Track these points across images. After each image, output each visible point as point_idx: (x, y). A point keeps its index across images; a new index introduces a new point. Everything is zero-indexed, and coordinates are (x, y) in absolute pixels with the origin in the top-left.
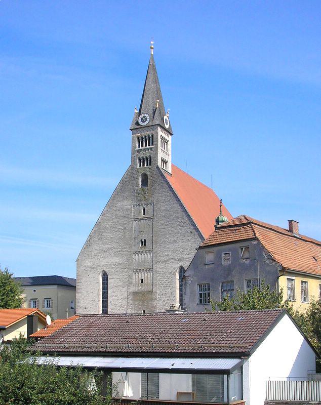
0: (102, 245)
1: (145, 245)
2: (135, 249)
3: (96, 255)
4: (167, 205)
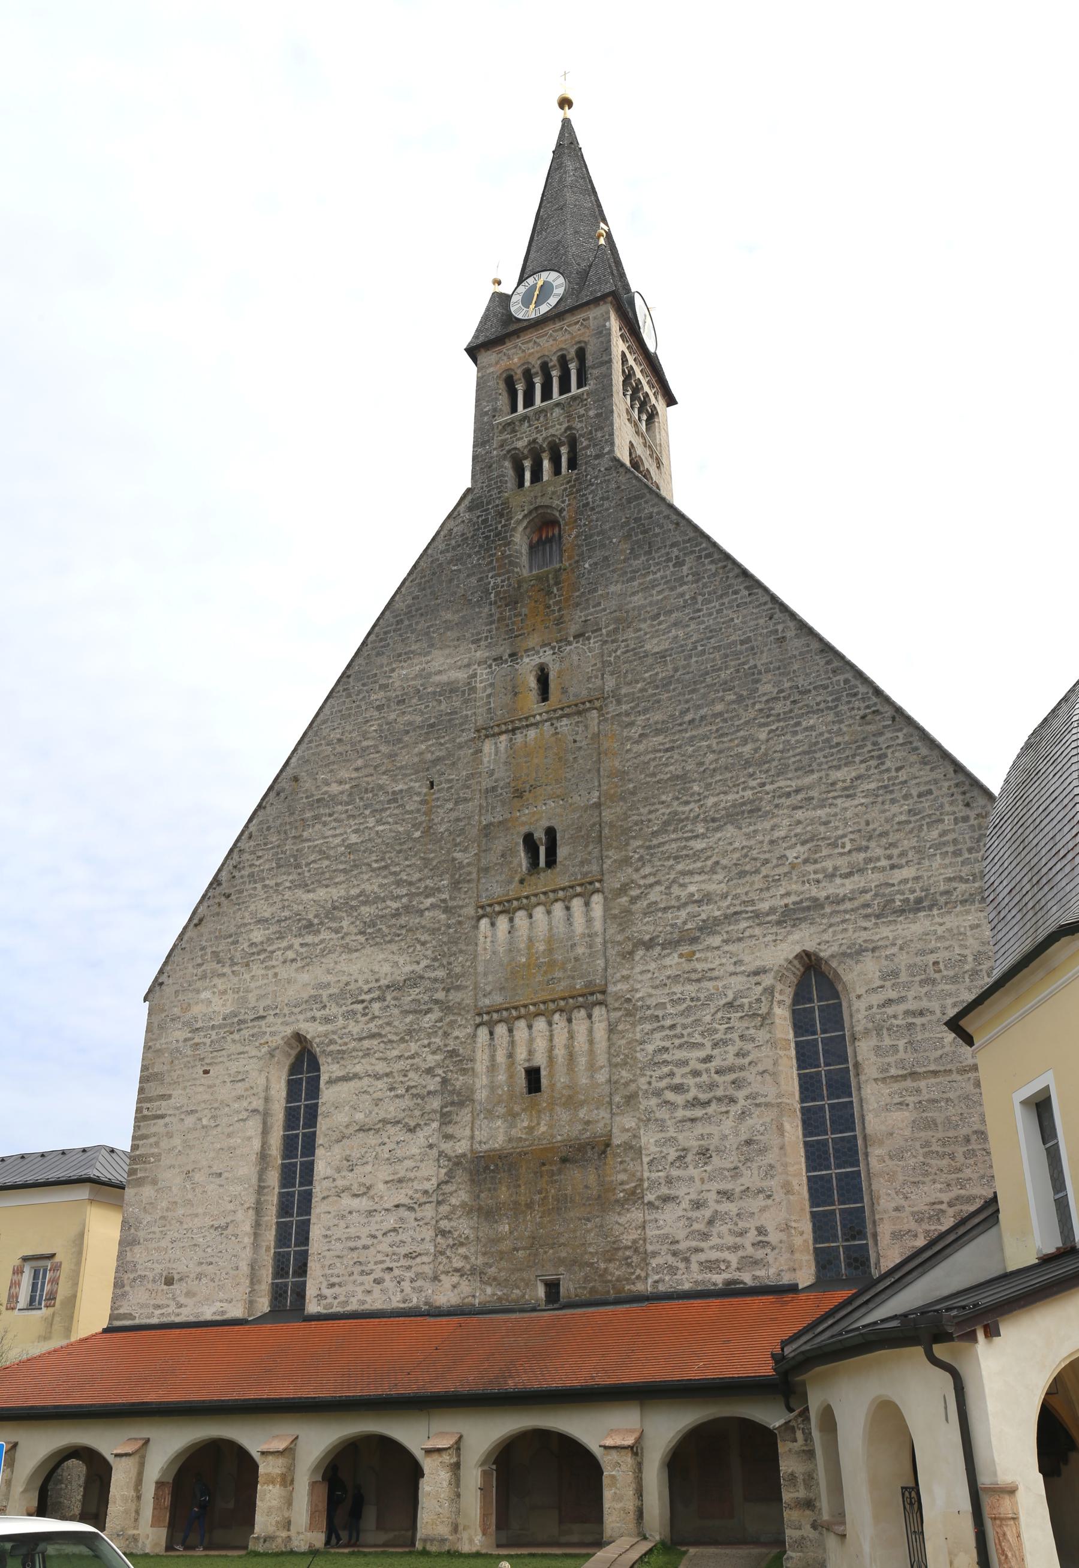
0: (299, 893)
1: (551, 862)
2: (495, 888)
3: (259, 950)
4: (675, 624)
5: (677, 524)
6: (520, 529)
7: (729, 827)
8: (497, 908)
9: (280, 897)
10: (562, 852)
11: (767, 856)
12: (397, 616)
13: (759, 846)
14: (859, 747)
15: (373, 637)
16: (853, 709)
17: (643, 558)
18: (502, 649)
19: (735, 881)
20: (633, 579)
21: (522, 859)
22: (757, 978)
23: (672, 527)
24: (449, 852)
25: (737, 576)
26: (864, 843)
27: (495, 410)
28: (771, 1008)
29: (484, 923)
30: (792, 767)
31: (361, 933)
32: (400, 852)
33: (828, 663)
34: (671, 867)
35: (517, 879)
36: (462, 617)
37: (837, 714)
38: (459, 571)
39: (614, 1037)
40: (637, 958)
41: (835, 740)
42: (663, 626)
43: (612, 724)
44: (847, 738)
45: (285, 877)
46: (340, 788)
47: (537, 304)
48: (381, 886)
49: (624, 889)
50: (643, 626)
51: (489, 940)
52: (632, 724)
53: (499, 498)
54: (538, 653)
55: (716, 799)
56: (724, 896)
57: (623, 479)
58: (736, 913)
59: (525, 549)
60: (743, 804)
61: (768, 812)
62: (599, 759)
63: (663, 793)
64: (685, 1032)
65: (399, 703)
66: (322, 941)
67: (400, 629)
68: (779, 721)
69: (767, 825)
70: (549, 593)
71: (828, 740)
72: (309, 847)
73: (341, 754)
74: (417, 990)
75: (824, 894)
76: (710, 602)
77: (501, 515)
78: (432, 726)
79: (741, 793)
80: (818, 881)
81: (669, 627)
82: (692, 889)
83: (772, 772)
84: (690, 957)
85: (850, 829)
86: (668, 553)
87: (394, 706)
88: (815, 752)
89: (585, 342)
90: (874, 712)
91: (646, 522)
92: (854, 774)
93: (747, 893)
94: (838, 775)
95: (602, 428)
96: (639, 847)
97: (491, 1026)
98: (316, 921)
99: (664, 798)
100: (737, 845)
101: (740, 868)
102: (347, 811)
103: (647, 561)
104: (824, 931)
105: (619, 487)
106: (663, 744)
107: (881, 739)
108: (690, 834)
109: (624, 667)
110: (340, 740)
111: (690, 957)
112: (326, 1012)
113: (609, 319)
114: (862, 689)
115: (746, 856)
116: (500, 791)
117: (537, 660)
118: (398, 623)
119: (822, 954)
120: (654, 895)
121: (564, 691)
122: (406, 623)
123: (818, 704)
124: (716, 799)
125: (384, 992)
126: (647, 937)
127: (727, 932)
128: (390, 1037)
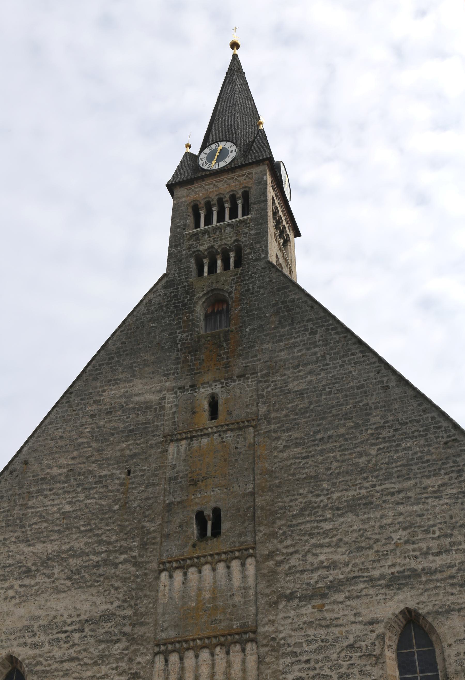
0: (22, 546)
1: (216, 532)
2: (173, 549)
4: (310, 373)
5: (312, 307)
6: (200, 303)
7: (350, 515)
8: (175, 565)
9: (6, 548)
10: (225, 526)
11: (378, 537)
12: (109, 354)
13: (372, 529)
14: (443, 464)
15: (90, 367)
16: (438, 437)
17: (288, 327)
18: (185, 381)
19: (354, 554)
20: (280, 341)
21: (194, 529)
22: (372, 627)
23: (308, 308)
24: (139, 521)
25: (354, 344)
26: (449, 531)
27: (185, 225)
28: (383, 650)
29: (164, 575)
30: (395, 475)
31: (69, 578)
32: (102, 520)
33: (420, 405)
34: (307, 541)
35: (191, 543)
36: (157, 358)
37: (427, 440)
38: (156, 327)
39: (263, 667)
40: (281, 607)
41: (426, 458)
42: (301, 374)
43: (264, 437)
44: (434, 457)
45: (12, 534)
46: (60, 471)
47: (218, 161)
48: (86, 544)
49: (271, 555)
50: (287, 372)
51: (167, 588)
52: (278, 438)
53: (186, 282)
54: (211, 386)
55: (339, 494)
56: (346, 564)
57: (274, 275)
58: (355, 577)
59: (202, 317)
60: (360, 498)
61: (378, 505)
62: (254, 461)
63: (301, 488)
64: (317, 666)
65: (107, 414)
66: (37, 584)
67: (111, 363)
68: (385, 442)
69: (378, 514)
70: (220, 346)
71: (421, 458)
72: (32, 513)
73: (62, 447)
74: (110, 624)
75: (420, 567)
76: (335, 359)
77: (187, 293)
78: (131, 431)
79: (358, 491)
80: (416, 557)
81: (306, 374)
82: (322, 557)
83: (381, 478)
84: (320, 608)
85: (438, 521)
86: (305, 326)
87: (103, 416)
88: (411, 465)
89: (249, 188)
90: (453, 440)
91: (290, 304)
92: (440, 482)
93: (363, 563)
94: (429, 482)
95: (260, 242)
96: (283, 525)
97: (166, 655)
98: (33, 568)
99: (301, 491)
100: (355, 527)
101: (358, 545)
102: (63, 488)
103: (291, 329)
104: (422, 594)
105: (271, 281)
106: (301, 453)
107: (459, 459)
108: (320, 518)
109: (273, 400)
110: (61, 437)
111: (320, 608)
112: (36, 639)
113: (266, 174)
114: (444, 424)
115: (362, 536)
116: (180, 480)
117: (209, 391)
118: (109, 359)
119: (420, 611)
120: (294, 561)
121: (229, 413)
122: (116, 359)
123: (413, 432)
124: (339, 494)
125: (83, 625)
126: (288, 592)
127: (349, 591)
128: (86, 661)
